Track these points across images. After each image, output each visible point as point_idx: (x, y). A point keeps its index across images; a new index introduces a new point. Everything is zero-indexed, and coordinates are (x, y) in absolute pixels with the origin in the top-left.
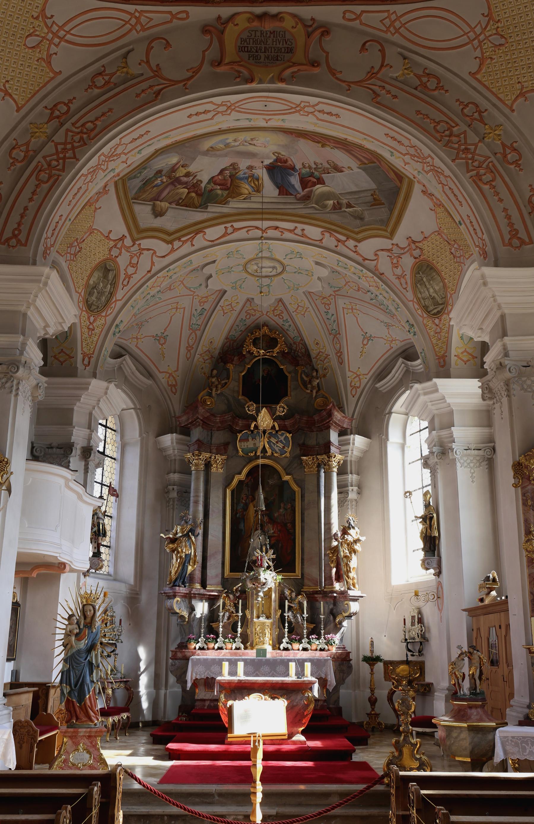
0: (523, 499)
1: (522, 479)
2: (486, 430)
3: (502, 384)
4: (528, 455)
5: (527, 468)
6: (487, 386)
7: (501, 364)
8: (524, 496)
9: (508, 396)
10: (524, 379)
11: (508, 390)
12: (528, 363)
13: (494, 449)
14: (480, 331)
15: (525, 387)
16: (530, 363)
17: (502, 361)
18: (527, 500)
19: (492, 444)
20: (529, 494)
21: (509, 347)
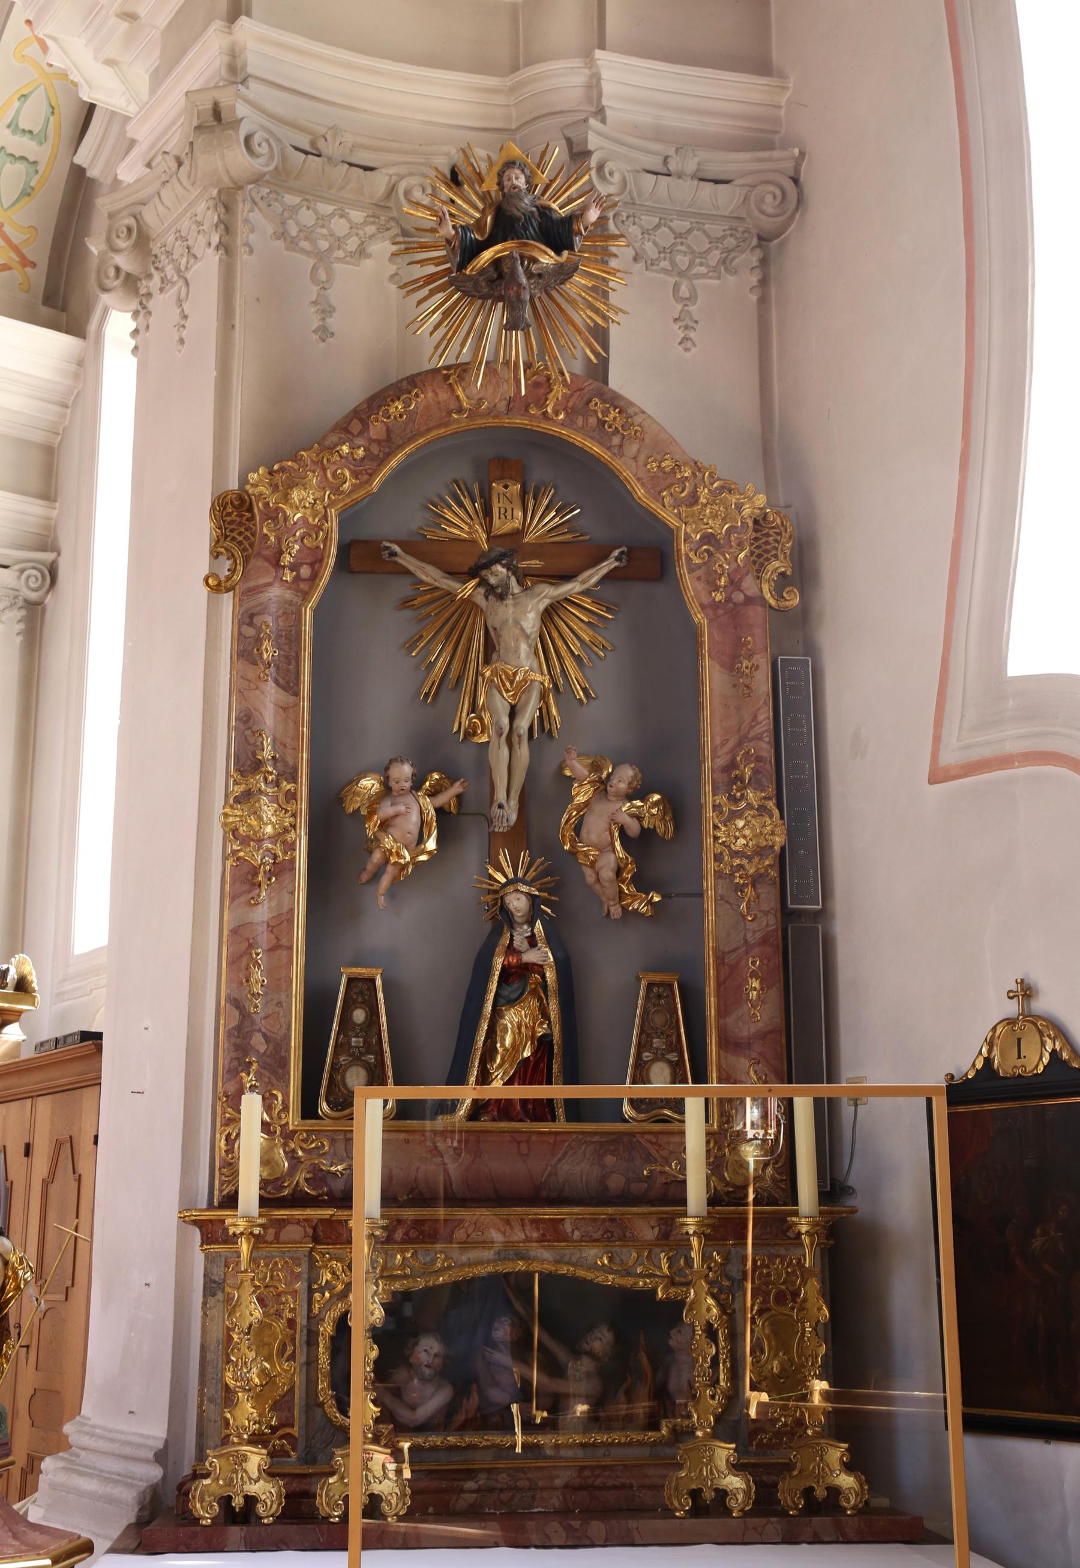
0: (240, 637)
1: (246, 560)
2: (35, 508)
3: (201, 207)
4: (282, 469)
5: (275, 519)
6: (131, 221)
7: (217, 113)
8: (251, 624)
9: (226, 248)
10: (291, 199)
11: (227, 228)
12: (313, 144)
13: (53, 572)
14: (124, 25)
15: (293, 231)
16: (321, 144)
17: (225, 98)
18: (258, 641)
19: (49, 557)
20: (269, 619)
21: (254, 64)
